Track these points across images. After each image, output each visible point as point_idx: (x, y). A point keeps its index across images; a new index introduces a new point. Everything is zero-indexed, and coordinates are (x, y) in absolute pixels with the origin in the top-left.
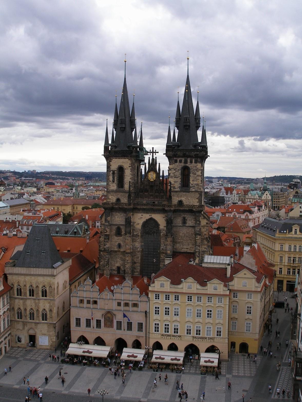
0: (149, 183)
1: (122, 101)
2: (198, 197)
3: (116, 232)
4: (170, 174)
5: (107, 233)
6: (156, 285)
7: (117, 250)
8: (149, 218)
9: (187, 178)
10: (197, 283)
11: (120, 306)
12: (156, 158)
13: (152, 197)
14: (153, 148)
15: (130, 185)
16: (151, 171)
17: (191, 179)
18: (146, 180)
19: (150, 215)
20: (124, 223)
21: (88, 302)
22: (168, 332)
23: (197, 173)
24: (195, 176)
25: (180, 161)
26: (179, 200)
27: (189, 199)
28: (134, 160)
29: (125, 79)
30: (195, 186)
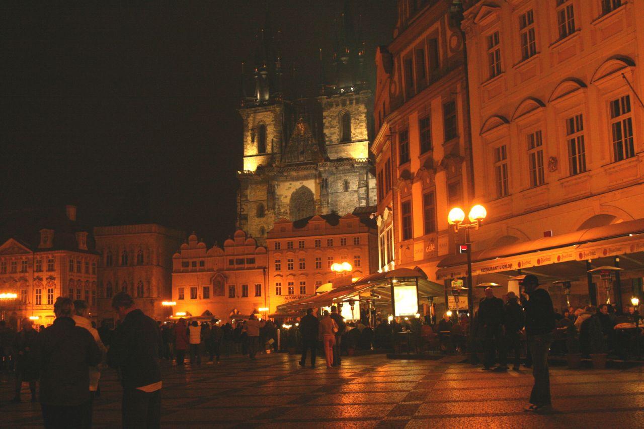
3: (257, 213)
4: (325, 123)
5: (245, 213)
7: (259, 236)
8: (300, 186)
10: (326, 222)
11: (233, 264)
13: (302, 158)
15: (272, 145)
17: (352, 127)
19: (301, 182)
20: (266, 199)
21: (194, 264)
22: (293, 293)
24: (358, 122)
25: (337, 105)
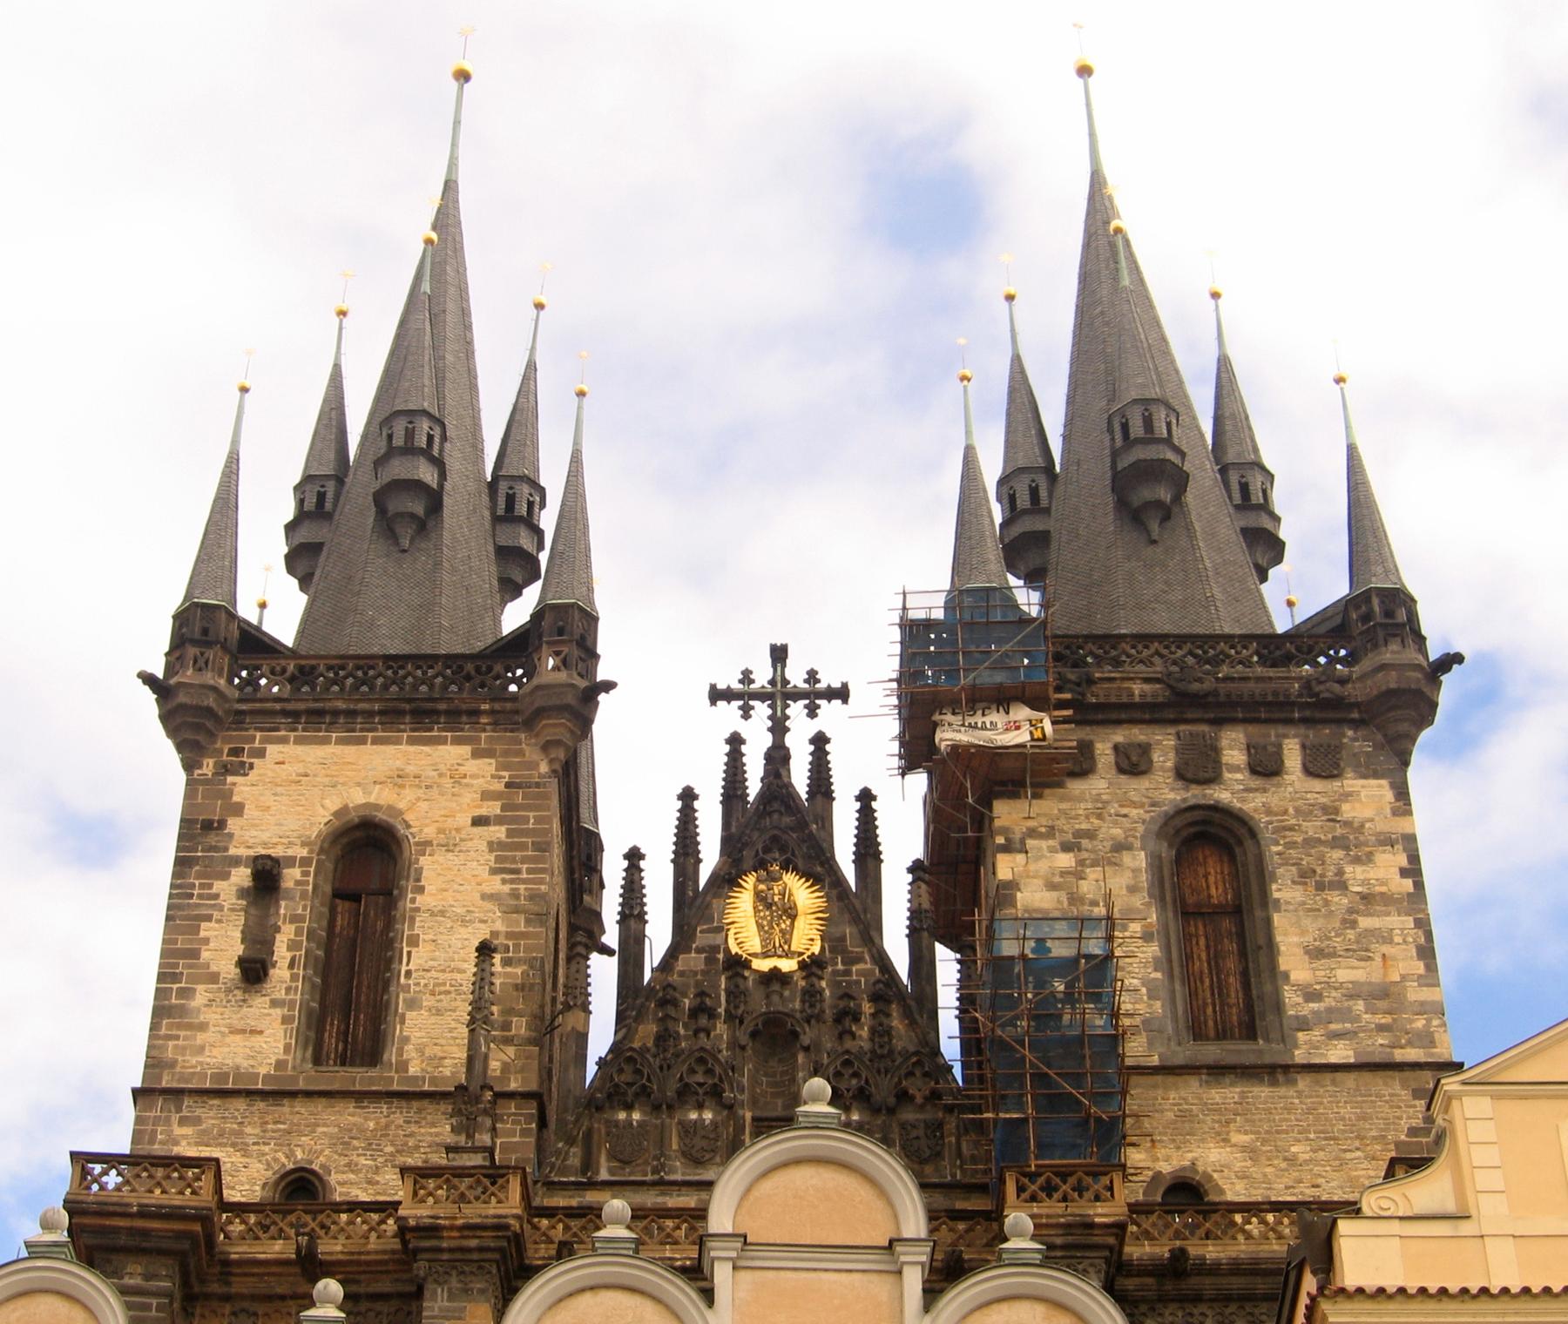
0: (734, 994)
1: (426, 287)
2: (1404, 1124)
4: (1012, 886)
6: (1483, 1180)
9: (1231, 946)
12: (820, 741)
14: (779, 654)
15: (483, 978)
16: (760, 865)
18: (692, 961)
23: (1356, 875)
24: (1339, 901)
25: (1133, 763)
26: (1165, 1168)
27: (1292, 1160)
28: (546, 747)
29: (450, 187)
30: (1360, 1006)
